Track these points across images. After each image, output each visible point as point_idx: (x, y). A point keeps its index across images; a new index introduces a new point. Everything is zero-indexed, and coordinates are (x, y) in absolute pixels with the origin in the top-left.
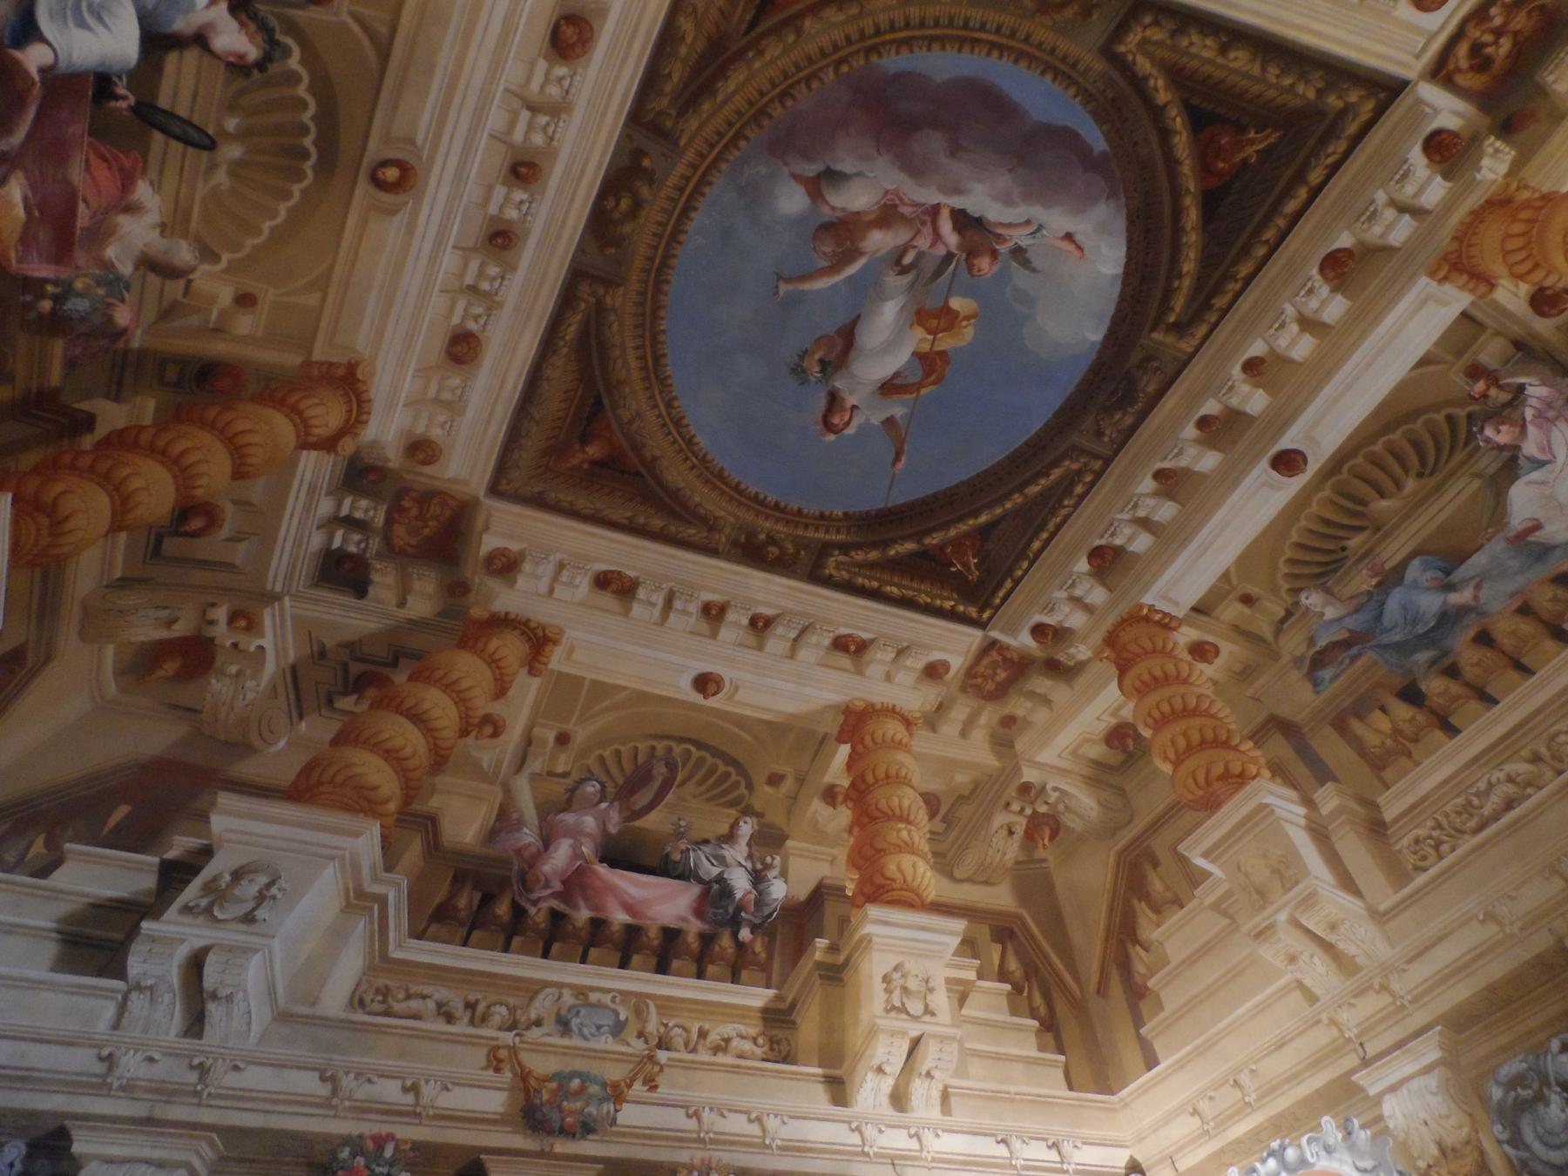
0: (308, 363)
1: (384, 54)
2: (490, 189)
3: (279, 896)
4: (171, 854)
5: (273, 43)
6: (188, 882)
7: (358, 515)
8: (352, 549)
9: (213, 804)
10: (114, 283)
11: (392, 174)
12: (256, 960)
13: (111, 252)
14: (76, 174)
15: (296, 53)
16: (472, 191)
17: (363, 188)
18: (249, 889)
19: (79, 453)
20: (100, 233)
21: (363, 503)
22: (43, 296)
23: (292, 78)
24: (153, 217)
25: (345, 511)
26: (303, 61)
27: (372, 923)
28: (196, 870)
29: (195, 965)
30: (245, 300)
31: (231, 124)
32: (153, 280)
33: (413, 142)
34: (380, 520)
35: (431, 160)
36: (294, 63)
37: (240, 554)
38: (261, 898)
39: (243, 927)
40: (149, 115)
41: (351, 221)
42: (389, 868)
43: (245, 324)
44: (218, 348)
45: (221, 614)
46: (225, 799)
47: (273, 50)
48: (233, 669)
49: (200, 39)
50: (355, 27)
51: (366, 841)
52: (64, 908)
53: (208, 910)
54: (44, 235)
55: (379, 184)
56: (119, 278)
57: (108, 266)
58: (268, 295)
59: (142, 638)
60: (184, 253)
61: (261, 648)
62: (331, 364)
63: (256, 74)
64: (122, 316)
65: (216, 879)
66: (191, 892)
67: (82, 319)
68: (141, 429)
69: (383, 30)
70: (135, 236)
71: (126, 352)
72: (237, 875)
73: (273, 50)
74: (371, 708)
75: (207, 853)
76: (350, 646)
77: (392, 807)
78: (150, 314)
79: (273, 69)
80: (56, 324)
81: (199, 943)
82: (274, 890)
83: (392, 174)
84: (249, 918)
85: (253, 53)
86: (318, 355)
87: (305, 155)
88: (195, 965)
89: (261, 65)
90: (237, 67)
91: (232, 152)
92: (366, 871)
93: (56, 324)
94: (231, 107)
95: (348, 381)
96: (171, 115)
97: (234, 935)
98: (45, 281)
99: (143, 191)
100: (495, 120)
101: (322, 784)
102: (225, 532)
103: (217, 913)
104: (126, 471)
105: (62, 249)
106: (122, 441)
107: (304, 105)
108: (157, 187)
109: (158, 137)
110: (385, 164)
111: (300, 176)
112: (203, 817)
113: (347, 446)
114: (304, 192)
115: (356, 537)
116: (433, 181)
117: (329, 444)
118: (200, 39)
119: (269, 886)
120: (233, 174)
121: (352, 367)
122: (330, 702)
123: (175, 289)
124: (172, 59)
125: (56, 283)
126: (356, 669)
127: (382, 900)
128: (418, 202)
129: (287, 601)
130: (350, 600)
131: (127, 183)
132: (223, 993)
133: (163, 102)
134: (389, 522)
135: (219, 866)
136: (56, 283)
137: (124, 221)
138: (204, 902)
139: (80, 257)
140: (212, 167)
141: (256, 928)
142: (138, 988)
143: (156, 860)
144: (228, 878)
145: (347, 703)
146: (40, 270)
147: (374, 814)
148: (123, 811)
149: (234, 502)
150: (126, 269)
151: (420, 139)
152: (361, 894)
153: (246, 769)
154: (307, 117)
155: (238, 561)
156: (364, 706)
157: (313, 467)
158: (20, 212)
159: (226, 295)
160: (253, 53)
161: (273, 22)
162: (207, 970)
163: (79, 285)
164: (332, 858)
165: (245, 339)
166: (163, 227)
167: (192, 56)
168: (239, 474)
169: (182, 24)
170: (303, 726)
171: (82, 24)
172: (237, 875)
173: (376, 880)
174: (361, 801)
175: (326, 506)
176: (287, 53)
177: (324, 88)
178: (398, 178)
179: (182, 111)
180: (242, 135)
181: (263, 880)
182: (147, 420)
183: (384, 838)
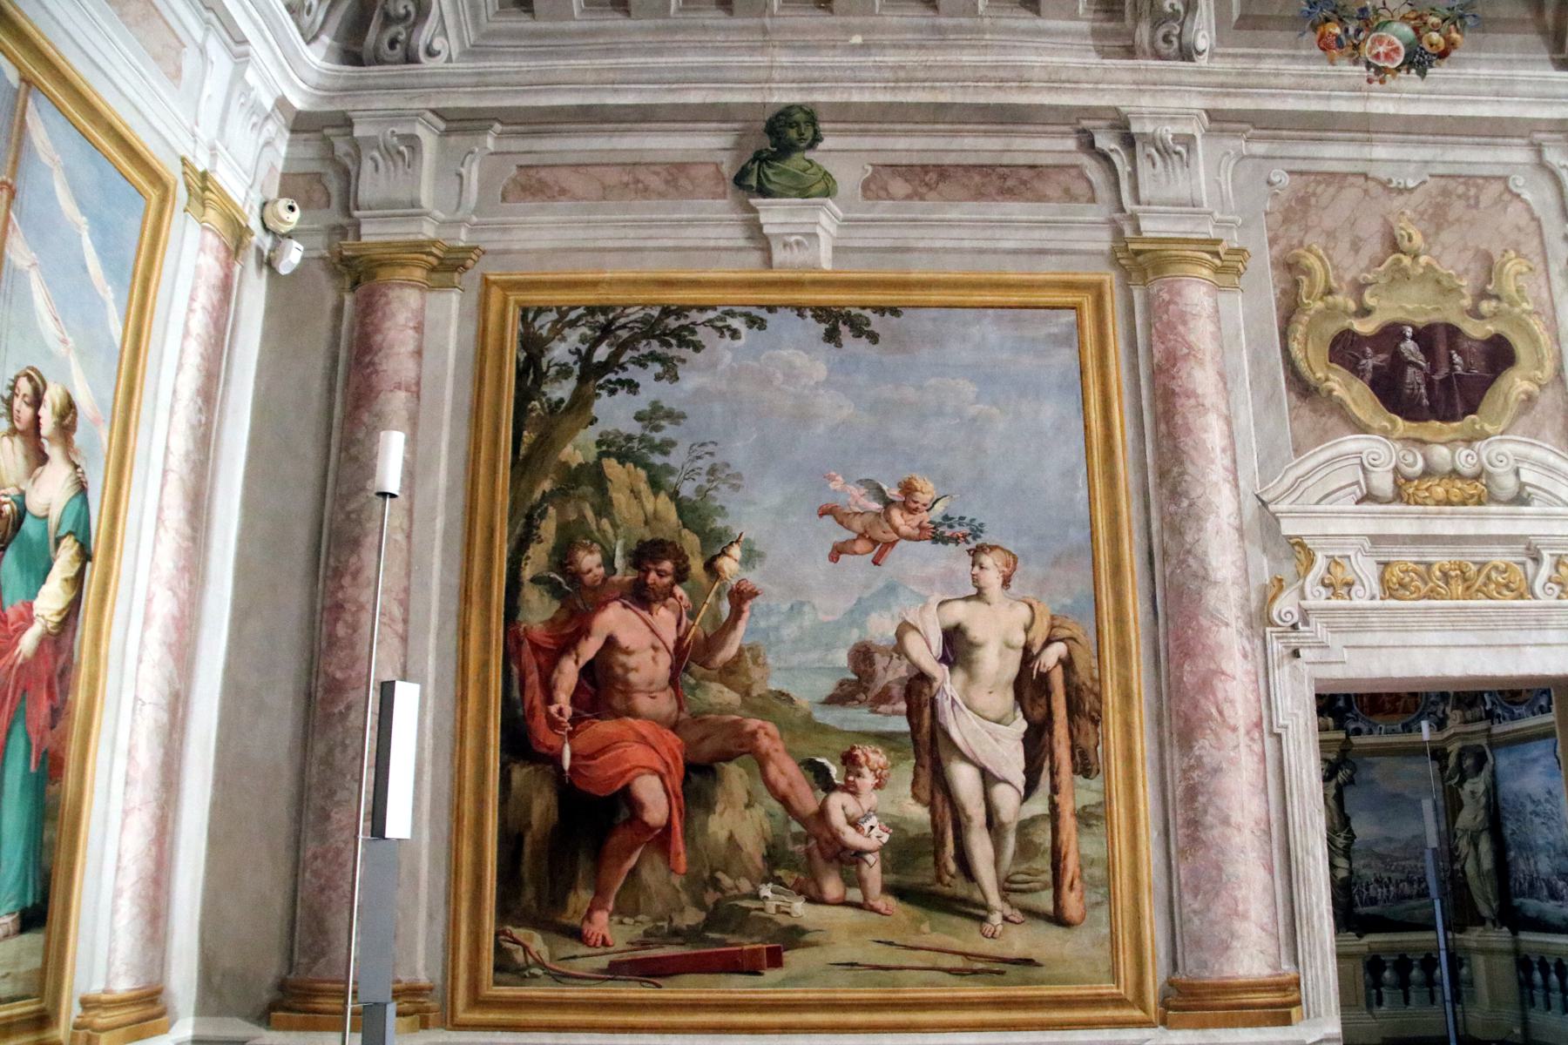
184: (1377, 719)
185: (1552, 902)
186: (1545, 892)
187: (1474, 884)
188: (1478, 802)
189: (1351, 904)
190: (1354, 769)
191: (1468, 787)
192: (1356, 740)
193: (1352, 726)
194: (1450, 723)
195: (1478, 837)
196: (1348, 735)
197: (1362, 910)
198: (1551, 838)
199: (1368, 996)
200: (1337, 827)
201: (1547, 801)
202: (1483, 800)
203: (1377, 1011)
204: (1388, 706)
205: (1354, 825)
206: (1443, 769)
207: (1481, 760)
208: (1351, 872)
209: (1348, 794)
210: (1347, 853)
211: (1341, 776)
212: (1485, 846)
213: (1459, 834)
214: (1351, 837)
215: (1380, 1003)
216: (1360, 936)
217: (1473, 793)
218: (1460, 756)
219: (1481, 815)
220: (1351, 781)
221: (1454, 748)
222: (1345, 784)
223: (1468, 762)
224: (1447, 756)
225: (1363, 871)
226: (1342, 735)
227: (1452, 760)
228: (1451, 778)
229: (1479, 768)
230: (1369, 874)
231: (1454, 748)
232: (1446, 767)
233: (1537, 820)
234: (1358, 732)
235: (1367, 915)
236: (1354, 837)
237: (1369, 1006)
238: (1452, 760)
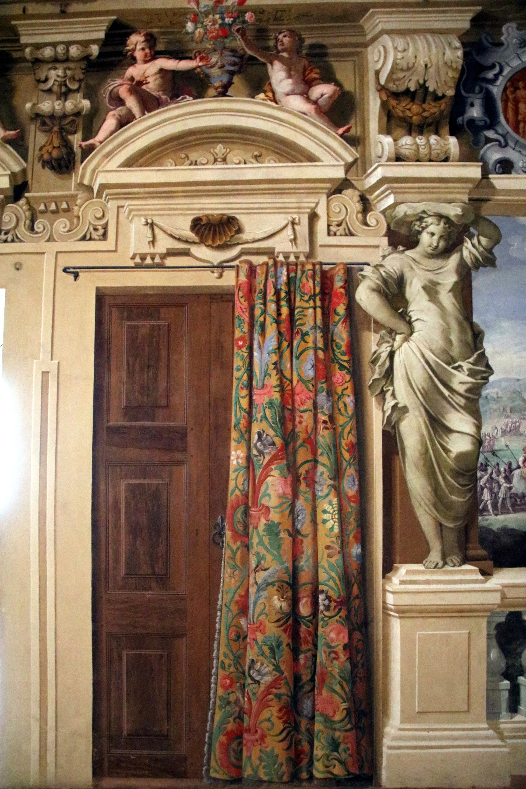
189: (474, 509)
190: (496, 239)
192: (500, 182)
193: (494, 155)
197: (494, 521)
199: (492, 690)
200: (456, 350)
203: (506, 723)
205: (489, 347)
208: (479, 442)
209: (480, 281)
210: (473, 404)
211: (469, 250)
214: (483, 370)
215: (514, 706)
216: (486, 573)
220: (488, 260)
222: (477, 264)
225: (501, 443)
226: (474, 171)
230: (511, 448)
234: (506, 167)
235: (506, 531)
236: (489, 370)
237: (492, 714)
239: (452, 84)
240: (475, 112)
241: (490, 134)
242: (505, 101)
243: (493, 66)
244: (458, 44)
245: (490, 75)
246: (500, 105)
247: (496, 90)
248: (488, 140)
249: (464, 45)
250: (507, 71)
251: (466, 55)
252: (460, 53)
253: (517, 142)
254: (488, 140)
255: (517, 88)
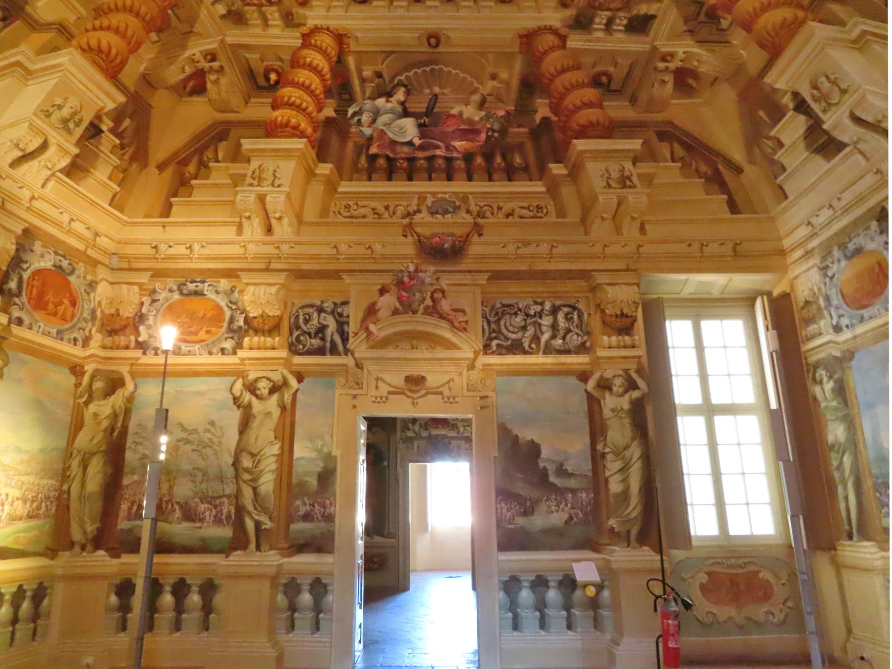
0: (521, 52)
1: (392, 53)
2: (429, 7)
3: (836, 76)
4: (791, 106)
5: (398, 85)
6: (809, 106)
7: (604, 21)
8: (625, 22)
9: (769, 85)
10: (488, 117)
11: (433, 41)
12: (870, 97)
13: (477, 118)
14: (451, 129)
15: (399, 78)
16: (433, 12)
17: (440, 49)
18: (825, 85)
19: (559, 120)
20: (470, 122)
21: (597, 20)
22: (492, 136)
23: (407, 77)
24: (463, 108)
25: (602, 27)
26: (401, 75)
27: (878, 42)
28: (804, 101)
29: (858, 121)
30: (494, 77)
31: (427, 91)
32: (486, 105)
33: (419, 37)
34: (608, 13)
35: (423, 29)
36: (403, 78)
37: (624, 63)
38: (834, 83)
39: (847, 96)
40: (429, 112)
41: (454, 50)
42: (843, 24)
43: (504, 75)
44: (515, 83)
45: (661, 65)
46: (768, 79)
47: (400, 84)
48: (695, 63)
49: (402, 104)
50: (386, 63)
51: (819, 31)
52: (802, 145)
53: (830, 104)
54: (471, 136)
55: (437, 45)
56: (486, 115)
57: (481, 119)
58: (490, 70)
59: (671, 91)
60: (476, 98)
61: (684, 53)
62: (521, 44)
63: (409, 87)
64: (502, 113)
65: (813, 96)
66: (815, 107)
67: (502, 124)
68: (551, 102)
69: (383, 55)
70: (470, 112)
71: (516, 110)
72: (815, 87)
73: (400, 84)
74: (730, 14)
75: (796, 95)
76: (686, 22)
77: (801, 14)
78: (500, 105)
79: (406, 83)
80: (503, 132)
81: (847, 113)
82: (832, 77)
83: (433, 41)
84: (844, 92)
85: (403, 89)
86: (517, 50)
87: (432, 70)
88: (858, 121)
89: (405, 86)
90: (408, 93)
91: (437, 90)
92: (839, 35)
93: (503, 132)
94: (421, 92)
95: (528, 38)
96: (427, 108)
97: (849, 102)
98: (487, 135)
99: (454, 111)
100: (401, 12)
101: (773, 43)
102: (611, 69)
103: (833, 102)
104: (571, 106)
105: (477, 132)
106: (555, 109)
107: (416, 73)
108: (452, 108)
109: (435, 110)
110: (429, 44)
111: (441, 69)
112: (775, 90)
113: (564, 31)
114: (446, 66)
115: (618, 21)
116: (434, 26)
117: (563, 39)
118: (402, 104)
119: (827, 77)
120: (444, 88)
121: (521, 37)
122: (722, 30)
123: (489, 98)
124: (409, 110)
125: (488, 132)
126: (702, 17)
127: (864, 33)
128: (440, 29)
129: (655, 43)
130: (657, 22)
131: (454, 116)
132: (880, 118)
133: (424, 110)
134: (609, 9)
135: (806, 93)
136: (488, 132)
137: (465, 116)
138: (824, 104)
139: (478, 127)
140: (443, 94)
141: (851, 92)
142: (856, 142)
143: (791, 112)
144: (815, 92)
145: (724, 24)
146: (483, 136)
147: (803, 22)
148: (761, 113)
149: (594, 66)
150: (483, 113)
151: (417, 35)
152: (855, 42)
153: (753, 69)
154: (419, 71)
155: (630, 62)
156: (729, 17)
157: (576, 41)
158: (464, 143)
159: (491, 84)
160: (403, 89)
161: (392, 85)
162: (864, 117)
163: (489, 126)
164: (823, 48)
165: (512, 74)
166: (466, 105)
167: (407, 105)
168: (578, 68)
169: (400, 109)
170: (734, 42)
171: (406, 131)
172: (815, 87)
173: (849, 32)
174: (792, 28)
175: (600, 34)
176: (400, 80)
177: (408, 68)
178: (434, 39)
179: (426, 105)
180: (430, 87)
181: (823, 79)
182: (547, 101)
183: (821, 21)
184: (38, 315)
185: (186, 525)
186: (178, 513)
187: (74, 505)
188: (99, 423)
191: (92, 408)
194: (92, 343)
195: (89, 459)
196: (9, 322)
198: (202, 464)
201: (208, 431)
202: (105, 424)
204: (51, 306)
206: (78, 385)
207: (114, 384)
212: (96, 467)
213: (75, 452)
217: (95, 415)
218: (93, 377)
219: (100, 436)
221: (89, 368)
223: (98, 385)
224: (84, 373)
227: (86, 380)
228: (81, 397)
229: (110, 392)
231: (89, 368)
232: (80, 384)
233: (188, 447)
234: (20, 322)
238: (86, 380)
239: (6, 264)
240: (13, 285)
241: (16, 300)
242: (28, 284)
243: (26, 262)
244: (14, 241)
245: (25, 266)
246: (25, 286)
247: (26, 276)
248: (15, 304)
249: (18, 244)
250: (32, 267)
251: (17, 250)
252: (14, 247)
253: (28, 310)
254: (15, 304)
255: (34, 279)
